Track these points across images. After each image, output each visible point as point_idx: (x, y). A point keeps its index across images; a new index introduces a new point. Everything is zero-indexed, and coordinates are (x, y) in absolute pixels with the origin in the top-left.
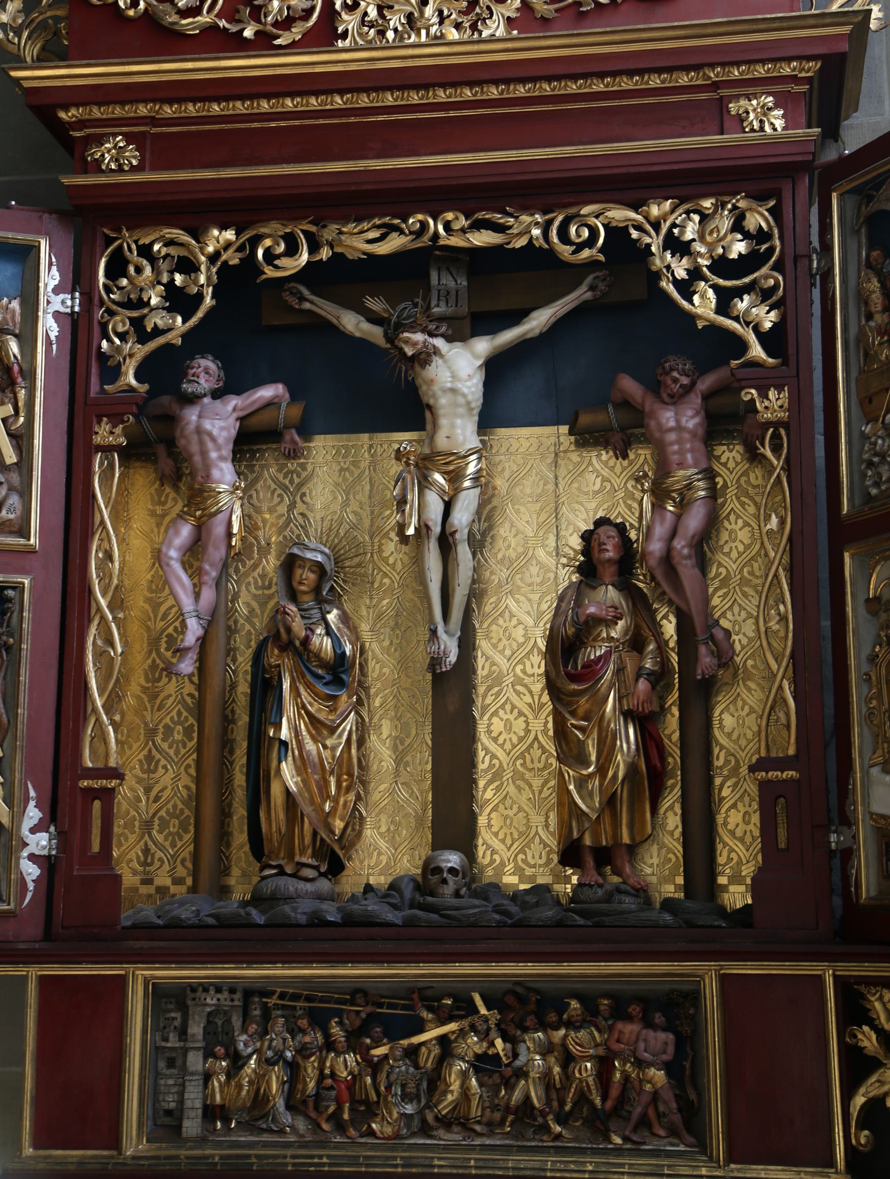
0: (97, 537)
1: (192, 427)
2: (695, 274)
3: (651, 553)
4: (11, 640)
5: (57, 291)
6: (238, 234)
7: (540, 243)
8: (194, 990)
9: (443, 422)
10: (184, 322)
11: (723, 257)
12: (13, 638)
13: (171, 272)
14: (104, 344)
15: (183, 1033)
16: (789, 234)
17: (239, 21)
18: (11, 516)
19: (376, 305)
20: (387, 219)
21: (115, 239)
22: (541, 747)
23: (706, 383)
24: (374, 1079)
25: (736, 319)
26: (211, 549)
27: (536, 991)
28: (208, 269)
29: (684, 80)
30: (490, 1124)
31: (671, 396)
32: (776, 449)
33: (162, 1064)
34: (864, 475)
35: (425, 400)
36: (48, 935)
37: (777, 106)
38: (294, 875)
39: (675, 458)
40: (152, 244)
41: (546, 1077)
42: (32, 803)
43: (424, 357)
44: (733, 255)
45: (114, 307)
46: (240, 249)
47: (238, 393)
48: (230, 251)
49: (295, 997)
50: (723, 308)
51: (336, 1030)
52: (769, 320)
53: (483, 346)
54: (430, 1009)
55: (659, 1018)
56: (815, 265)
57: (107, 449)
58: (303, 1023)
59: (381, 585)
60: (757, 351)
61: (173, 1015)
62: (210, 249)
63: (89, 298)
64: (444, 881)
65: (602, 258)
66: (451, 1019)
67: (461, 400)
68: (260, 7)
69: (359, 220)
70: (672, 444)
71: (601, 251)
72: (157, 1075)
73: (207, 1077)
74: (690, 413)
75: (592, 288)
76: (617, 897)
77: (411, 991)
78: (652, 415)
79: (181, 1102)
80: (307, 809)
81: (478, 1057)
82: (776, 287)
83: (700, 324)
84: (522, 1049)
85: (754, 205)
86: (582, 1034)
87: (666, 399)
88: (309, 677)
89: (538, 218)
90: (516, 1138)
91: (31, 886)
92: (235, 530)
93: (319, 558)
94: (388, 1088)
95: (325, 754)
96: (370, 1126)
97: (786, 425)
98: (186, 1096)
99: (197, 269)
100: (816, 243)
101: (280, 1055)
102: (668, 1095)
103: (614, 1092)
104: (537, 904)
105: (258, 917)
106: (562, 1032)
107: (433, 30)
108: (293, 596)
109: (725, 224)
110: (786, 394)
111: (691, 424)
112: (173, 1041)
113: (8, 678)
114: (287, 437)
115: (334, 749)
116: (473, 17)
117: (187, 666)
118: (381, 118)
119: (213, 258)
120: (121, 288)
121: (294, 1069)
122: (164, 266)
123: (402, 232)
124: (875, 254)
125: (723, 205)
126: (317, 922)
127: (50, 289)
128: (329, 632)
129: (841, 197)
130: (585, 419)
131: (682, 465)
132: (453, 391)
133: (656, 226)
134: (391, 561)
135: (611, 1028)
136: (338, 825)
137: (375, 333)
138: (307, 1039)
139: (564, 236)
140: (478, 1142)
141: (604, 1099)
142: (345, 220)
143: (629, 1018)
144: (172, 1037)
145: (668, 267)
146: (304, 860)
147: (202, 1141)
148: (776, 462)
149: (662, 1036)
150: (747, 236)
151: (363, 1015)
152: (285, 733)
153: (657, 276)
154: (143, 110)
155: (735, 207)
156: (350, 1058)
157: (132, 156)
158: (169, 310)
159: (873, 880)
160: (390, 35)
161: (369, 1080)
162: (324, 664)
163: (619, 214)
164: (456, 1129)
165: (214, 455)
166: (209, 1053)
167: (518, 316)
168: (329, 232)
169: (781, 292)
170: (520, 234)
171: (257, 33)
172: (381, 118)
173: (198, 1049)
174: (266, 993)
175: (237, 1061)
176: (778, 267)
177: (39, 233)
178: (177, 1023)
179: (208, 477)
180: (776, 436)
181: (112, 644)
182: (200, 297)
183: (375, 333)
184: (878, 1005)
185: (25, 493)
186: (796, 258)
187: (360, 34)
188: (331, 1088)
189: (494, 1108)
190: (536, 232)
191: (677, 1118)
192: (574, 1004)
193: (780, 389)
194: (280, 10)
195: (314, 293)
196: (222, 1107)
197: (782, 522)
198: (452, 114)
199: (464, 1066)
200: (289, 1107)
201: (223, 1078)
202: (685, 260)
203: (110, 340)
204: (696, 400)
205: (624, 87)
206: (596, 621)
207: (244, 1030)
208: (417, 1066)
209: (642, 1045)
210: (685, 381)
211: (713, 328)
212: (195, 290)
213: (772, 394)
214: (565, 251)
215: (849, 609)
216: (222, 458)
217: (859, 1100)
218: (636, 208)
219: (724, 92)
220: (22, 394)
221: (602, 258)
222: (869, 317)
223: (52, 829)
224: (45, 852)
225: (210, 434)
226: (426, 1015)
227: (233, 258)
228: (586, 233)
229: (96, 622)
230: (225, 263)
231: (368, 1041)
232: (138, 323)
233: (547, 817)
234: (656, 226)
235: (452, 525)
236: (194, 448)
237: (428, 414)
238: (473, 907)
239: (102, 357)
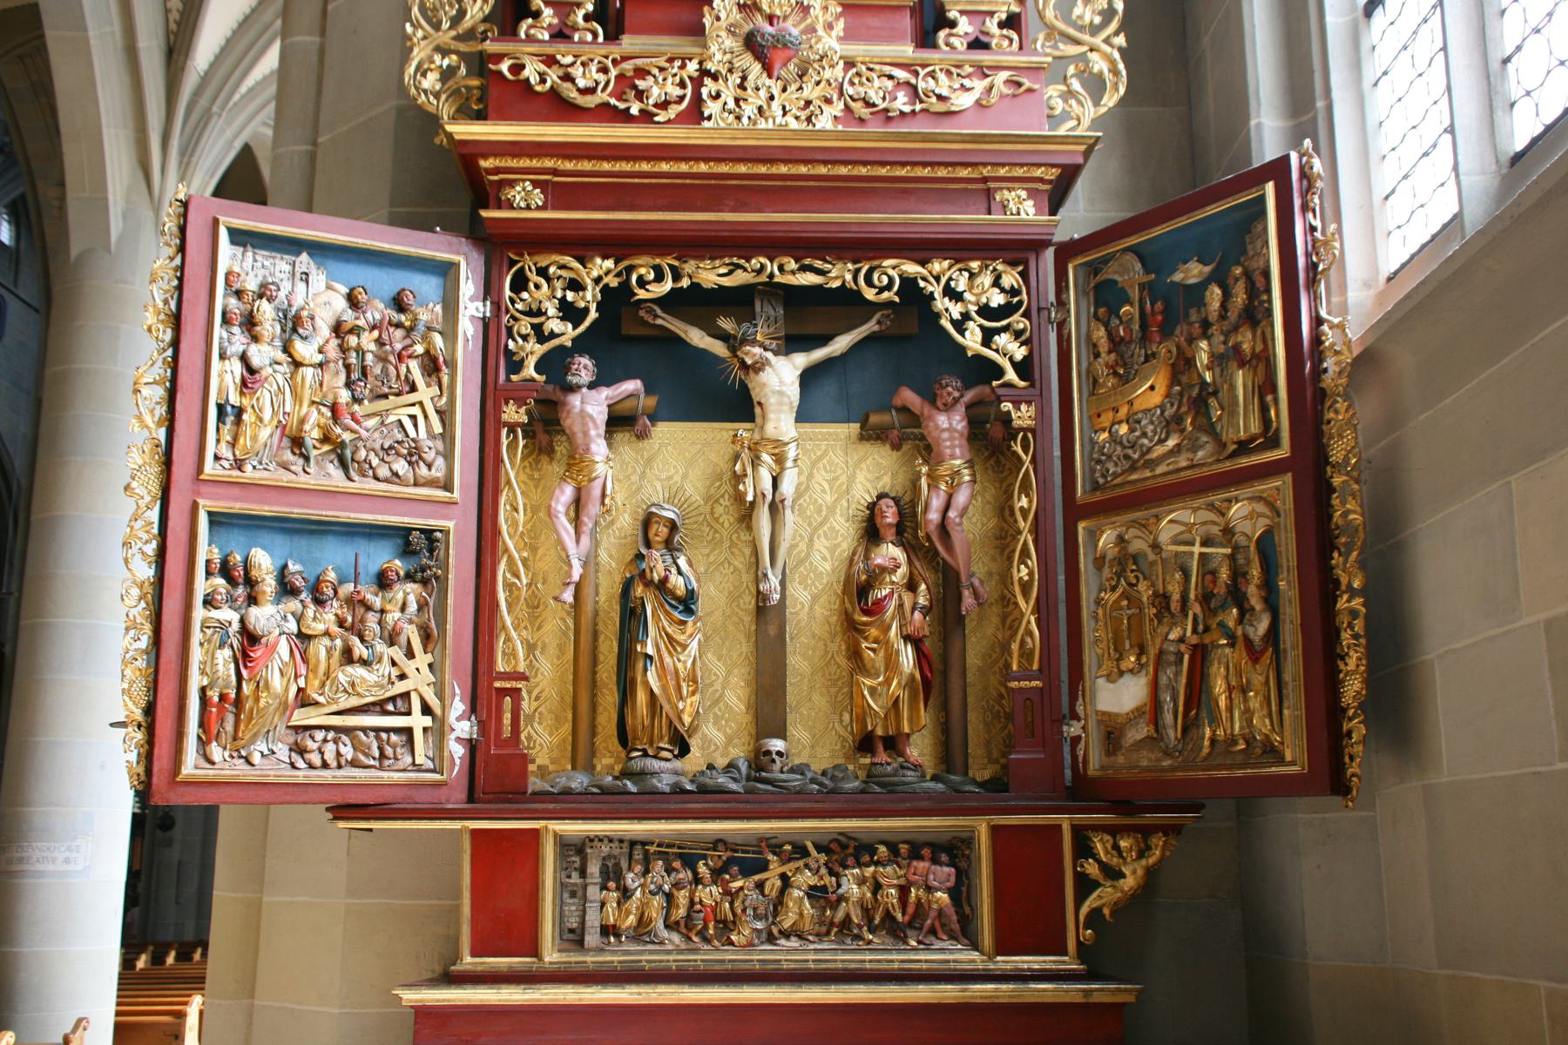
0: (505, 493)
1: (577, 410)
2: (966, 316)
3: (931, 521)
5: (472, 299)
6: (616, 263)
7: (850, 284)
8: (591, 840)
9: (771, 416)
10: (574, 328)
11: (987, 305)
13: (564, 290)
14: (511, 344)
15: (583, 873)
16: (1033, 292)
17: (626, 101)
18: (439, 475)
19: (726, 324)
20: (735, 260)
21: (515, 262)
22: (836, 663)
23: (969, 396)
24: (732, 904)
25: (997, 351)
26: (590, 506)
27: (855, 839)
28: (594, 289)
29: (964, 173)
30: (818, 935)
31: (945, 405)
32: (1026, 449)
33: (566, 895)
34: (1093, 471)
35: (756, 397)
36: (471, 798)
37: (1029, 197)
38: (655, 757)
39: (948, 451)
40: (547, 267)
41: (861, 903)
42: (457, 698)
43: (758, 367)
44: (994, 304)
45: (518, 315)
46: (618, 275)
47: (608, 385)
48: (610, 277)
49: (670, 846)
50: (987, 341)
51: (702, 869)
52: (1020, 353)
53: (801, 360)
54: (775, 853)
55: (944, 858)
56: (1053, 315)
57: (512, 428)
58: (677, 864)
59: (714, 538)
60: (1011, 375)
61: (573, 859)
62: (595, 274)
63: (497, 306)
64: (773, 761)
65: (897, 299)
66: (790, 860)
67: (786, 400)
68: (642, 92)
69: (713, 258)
70: (945, 440)
71: (896, 294)
72: (562, 903)
73: (603, 904)
74: (958, 418)
75: (879, 322)
76: (901, 772)
77: (761, 839)
78: (930, 418)
79: (583, 922)
80: (666, 707)
81: (812, 888)
82: (1022, 332)
83: (970, 354)
84: (844, 880)
85: (1009, 269)
86: (889, 869)
87: (941, 407)
88: (667, 607)
89: (850, 266)
90: (838, 943)
91: (458, 762)
92: (608, 492)
93: (671, 515)
94: (744, 911)
95: (680, 665)
96: (729, 938)
97: (1033, 431)
98: (587, 918)
99: (584, 289)
100: (1052, 298)
101: (660, 888)
102: (951, 911)
103: (910, 909)
104: (843, 778)
105: (631, 786)
106: (872, 869)
107: (778, 122)
108: (648, 545)
109: (986, 279)
110: (1032, 408)
111: (959, 427)
112: (575, 878)
114: (641, 422)
115: (685, 662)
116: (807, 112)
117: (568, 596)
118: (734, 182)
119: (597, 280)
120: (521, 300)
121: (669, 897)
122: (559, 284)
123: (745, 270)
124: (1102, 310)
125: (987, 267)
126: (678, 790)
127: (467, 297)
128: (680, 572)
129: (1075, 268)
130: (874, 419)
131: (953, 457)
132: (781, 393)
133: (937, 279)
134: (721, 520)
135: (909, 865)
136: (687, 719)
137: (719, 348)
138: (681, 876)
139: (869, 283)
140: (812, 947)
141: (904, 914)
142: (702, 258)
143: (921, 858)
144: (575, 875)
145: (947, 310)
146: (662, 745)
147: (601, 950)
148: (1024, 457)
149: (946, 869)
150: (1003, 290)
151: (724, 858)
152: (650, 650)
153: (938, 316)
154: (549, 163)
155: (995, 270)
156: (714, 888)
157: (538, 197)
158: (562, 319)
159: (1097, 757)
160: (745, 120)
161: (727, 905)
162: (678, 599)
163: (911, 268)
164: (793, 938)
165: (593, 433)
166: (604, 887)
167: (824, 340)
168: (689, 267)
169: (1028, 333)
170: (836, 278)
171: (641, 111)
172: (734, 182)
173: (596, 884)
174: (644, 844)
175: (626, 893)
176: (1026, 315)
177: (458, 253)
178: (577, 865)
179: (588, 450)
180: (1025, 438)
181: (518, 577)
182: (586, 311)
183: (719, 348)
184: (1099, 846)
185: (448, 455)
186: (1039, 309)
187: (722, 119)
188: (700, 911)
189: (821, 923)
190: (849, 277)
191: (956, 927)
192: (882, 849)
193: (1029, 403)
194: (660, 95)
195: (664, 311)
196: (614, 926)
197: (1030, 502)
198: (789, 183)
199: (801, 894)
200: (667, 926)
201: (615, 905)
202: (959, 304)
203: (514, 340)
204: (961, 408)
205: (919, 174)
206: (883, 569)
207: (630, 869)
208: (763, 895)
209: (931, 877)
210: (956, 394)
211: (978, 358)
212: (582, 305)
213: (1023, 407)
214: (870, 294)
215: (1082, 565)
216: (599, 436)
217: (1084, 910)
218: (923, 263)
219: (992, 185)
220: (445, 379)
221: (897, 299)
222: (1097, 355)
223: (473, 718)
224: (468, 737)
225: (591, 417)
226: (770, 857)
227: (614, 282)
228: (885, 280)
229: (505, 559)
230: (606, 285)
231: (727, 877)
232: (538, 328)
233: (841, 715)
234: (937, 279)
235: (782, 494)
236: (577, 428)
237: (757, 410)
238: (795, 781)
239: (509, 354)
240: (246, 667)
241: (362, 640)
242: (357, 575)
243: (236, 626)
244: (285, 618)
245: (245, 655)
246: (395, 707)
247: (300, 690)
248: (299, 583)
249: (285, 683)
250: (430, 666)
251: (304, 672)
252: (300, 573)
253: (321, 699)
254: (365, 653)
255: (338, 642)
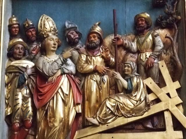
4: (179, 17)
12: (180, 16)
113: (180, 41)
240: (38, 100)
241: (124, 76)
242: (115, 26)
243: (29, 71)
244: (65, 62)
245: (38, 91)
246: (153, 124)
247: (78, 115)
248: (74, 35)
249: (66, 111)
250: (178, 90)
251: (79, 101)
252: (74, 28)
253: (95, 121)
254: (125, 83)
255: (106, 78)
